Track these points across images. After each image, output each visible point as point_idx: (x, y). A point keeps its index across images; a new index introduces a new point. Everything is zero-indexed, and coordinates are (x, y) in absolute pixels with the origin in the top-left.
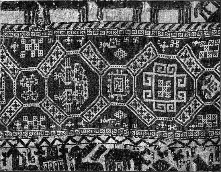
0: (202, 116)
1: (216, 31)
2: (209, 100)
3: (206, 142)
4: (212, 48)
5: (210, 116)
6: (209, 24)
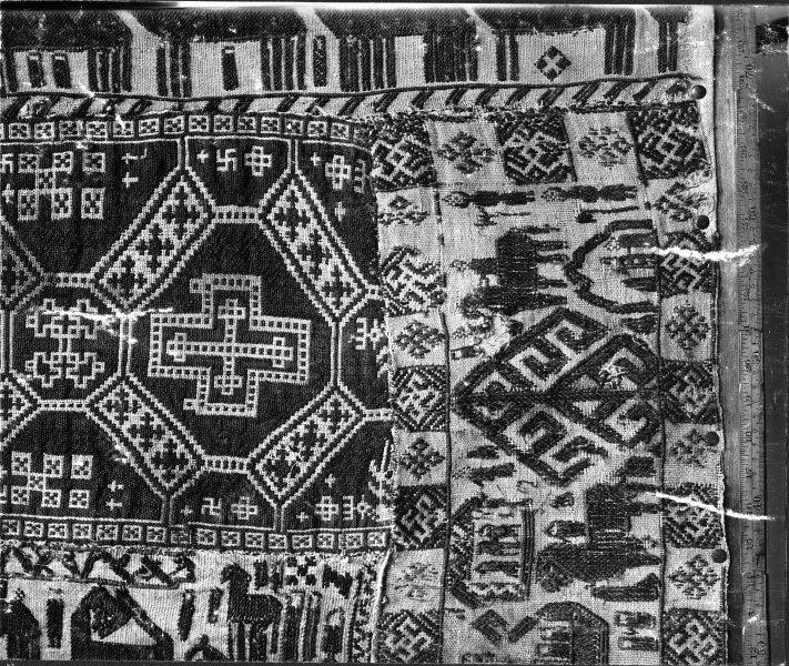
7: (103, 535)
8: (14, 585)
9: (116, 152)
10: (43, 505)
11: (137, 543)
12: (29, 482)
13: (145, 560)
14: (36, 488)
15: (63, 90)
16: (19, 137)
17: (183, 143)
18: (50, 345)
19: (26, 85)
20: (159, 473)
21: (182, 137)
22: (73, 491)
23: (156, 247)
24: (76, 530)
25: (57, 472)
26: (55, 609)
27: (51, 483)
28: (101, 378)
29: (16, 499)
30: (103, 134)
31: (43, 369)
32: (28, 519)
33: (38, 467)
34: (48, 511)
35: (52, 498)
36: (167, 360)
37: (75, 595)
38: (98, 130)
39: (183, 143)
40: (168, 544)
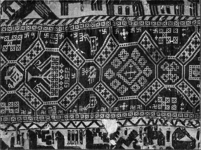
0: (5, 103)
1: (19, 27)
2: (11, 89)
3: (8, 127)
4: (14, 43)
5: (12, 103)
6: (13, 21)
7: (179, 116)
8: (159, 127)
9: (180, 28)
10: (165, 109)
11: (187, 118)
12: (162, 104)
13: (189, 122)
14: (164, 105)
15: (169, 14)
16: (159, 25)
17: (196, 26)
18: (166, 72)
19: (160, 14)
20: (192, 102)
21: (196, 25)
22: (172, 106)
23: (190, 50)
24: (173, 115)
25: (168, 101)
26: (168, 133)
27: (167, 104)
28: (178, 80)
29: (159, 108)
30: (178, 24)
31: (165, 78)
32: (162, 112)
33: (164, 100)
34: (167, 110)
35: (167, 107)
36: (193, 76)
37: (173, 130)
38: (176, 23)
39: (196, 26)
40: (194, 118)
